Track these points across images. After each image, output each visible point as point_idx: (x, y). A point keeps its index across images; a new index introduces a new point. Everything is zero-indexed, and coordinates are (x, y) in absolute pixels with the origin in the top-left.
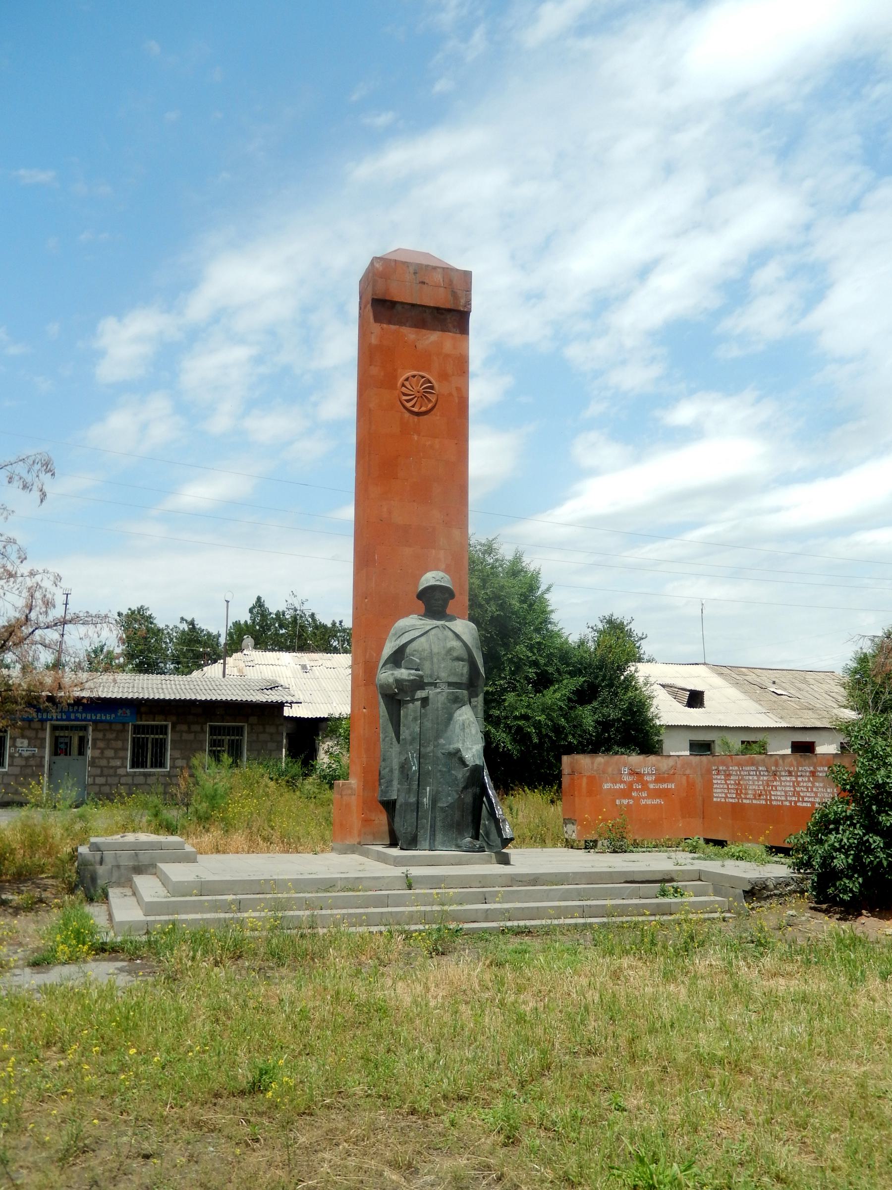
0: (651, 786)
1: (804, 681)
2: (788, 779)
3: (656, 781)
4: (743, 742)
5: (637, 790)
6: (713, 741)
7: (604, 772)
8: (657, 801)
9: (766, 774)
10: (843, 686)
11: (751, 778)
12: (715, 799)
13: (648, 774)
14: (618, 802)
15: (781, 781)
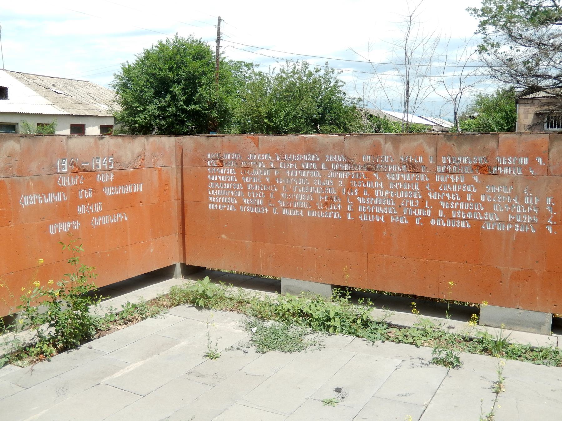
0: (109, 192)
1: (72, 86)
2: (408, 177)
3: (117, 182)
4: (38, 124)
5: (86, 201)
6: (17, 123)
7: (21, 172)
8: (119, 217)
9: (346, 167)
10: (114, 87)
11: (304, 174)
12: (211, 207)
13: (103, 170)
14: (52, 230)
15: (386, 182)
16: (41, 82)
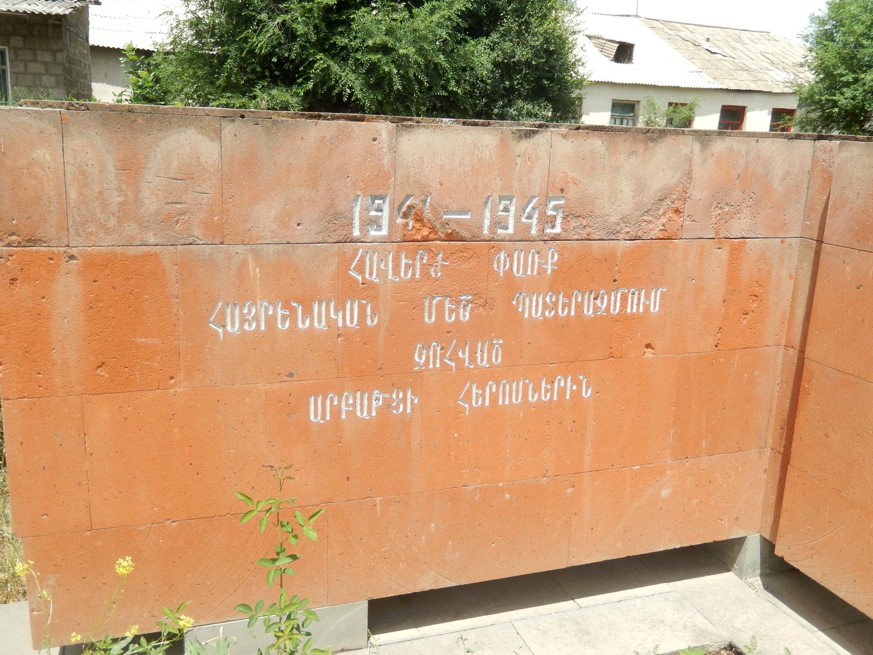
1: (739, 40)
3: (564, 280)
4: (670, 104)
5: (444, 334)
6: (638, 102)
7: (220, 233)
10: (806, 38)
13: (523, 238)
14: (317, 411)
16: (688, 33)
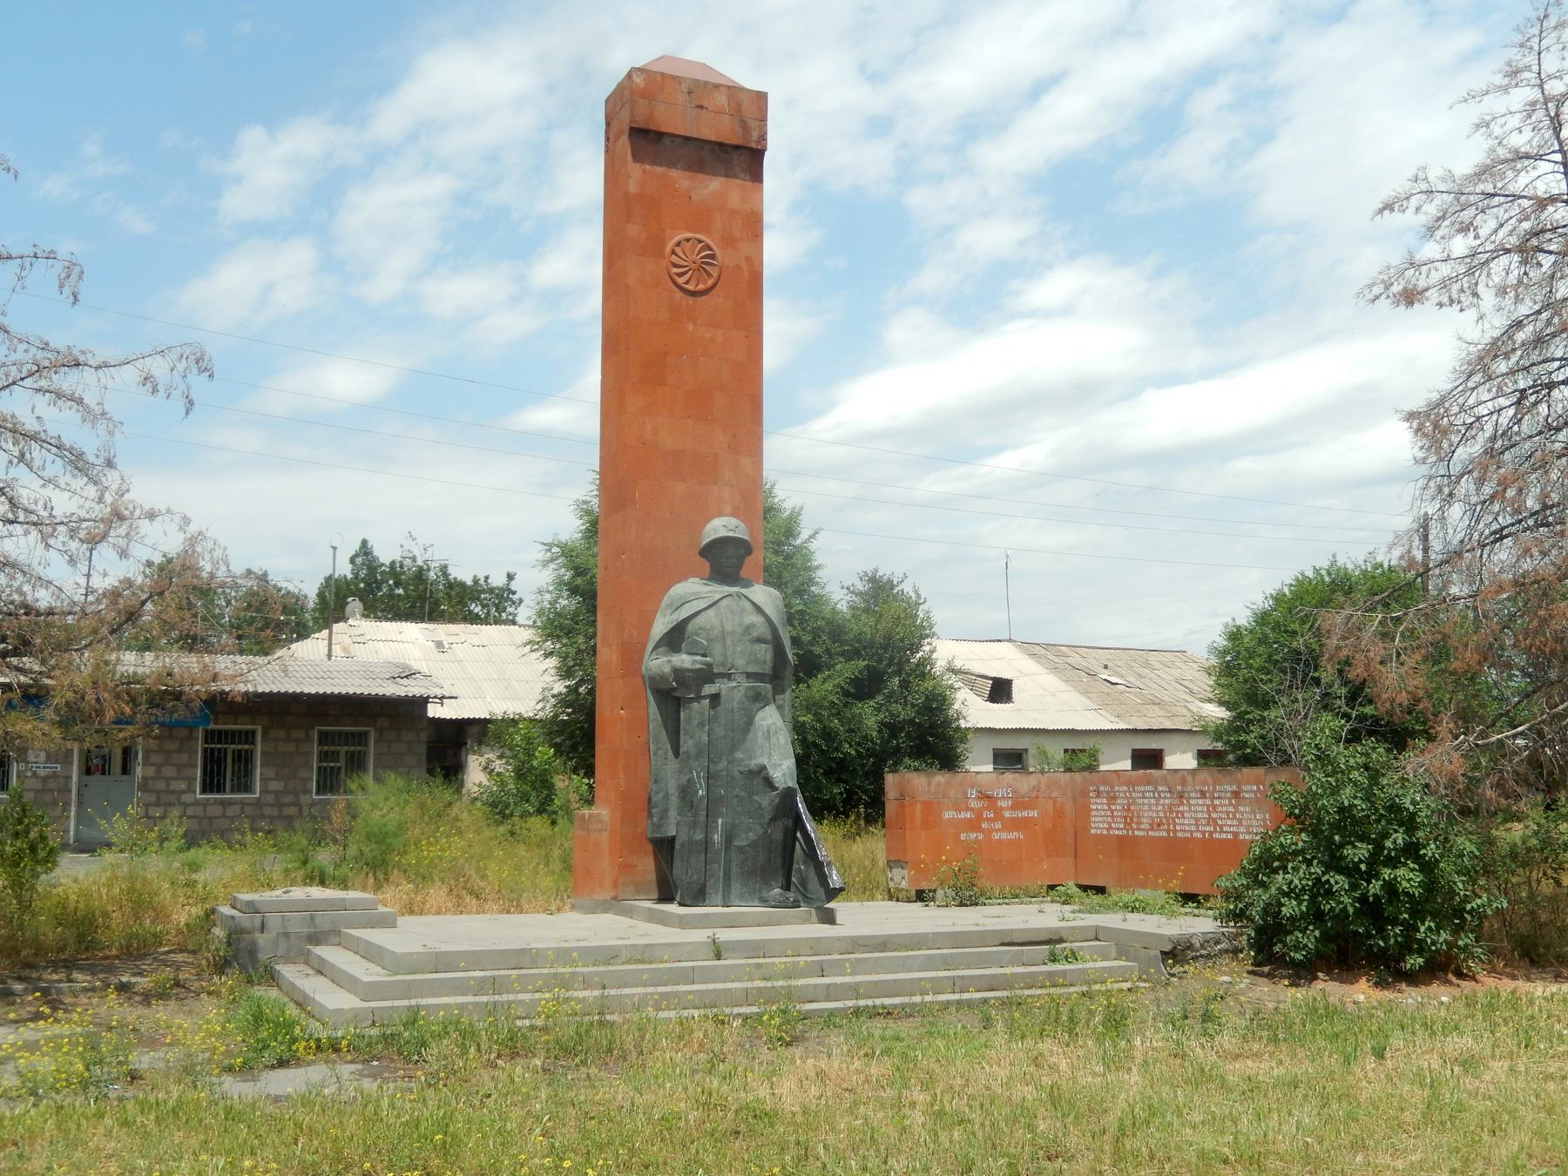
0: (1007, 814)
1: (1147, 665)
3: (1014, 807)
4: (1066, 751)
5: (988, 820)
6: (1026, 750)
15: (1190, 805)
16: (1079, 659)
